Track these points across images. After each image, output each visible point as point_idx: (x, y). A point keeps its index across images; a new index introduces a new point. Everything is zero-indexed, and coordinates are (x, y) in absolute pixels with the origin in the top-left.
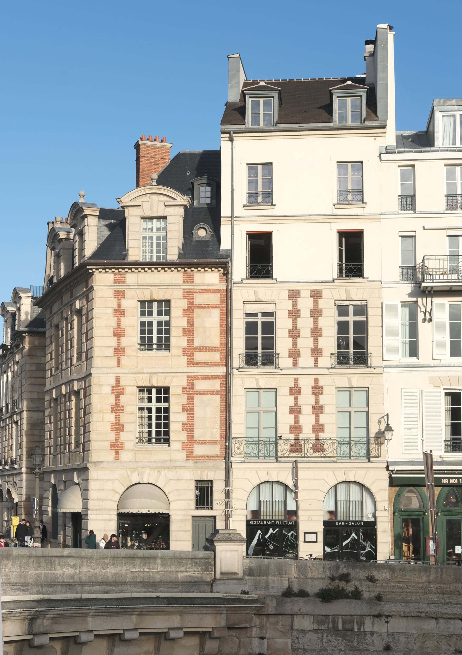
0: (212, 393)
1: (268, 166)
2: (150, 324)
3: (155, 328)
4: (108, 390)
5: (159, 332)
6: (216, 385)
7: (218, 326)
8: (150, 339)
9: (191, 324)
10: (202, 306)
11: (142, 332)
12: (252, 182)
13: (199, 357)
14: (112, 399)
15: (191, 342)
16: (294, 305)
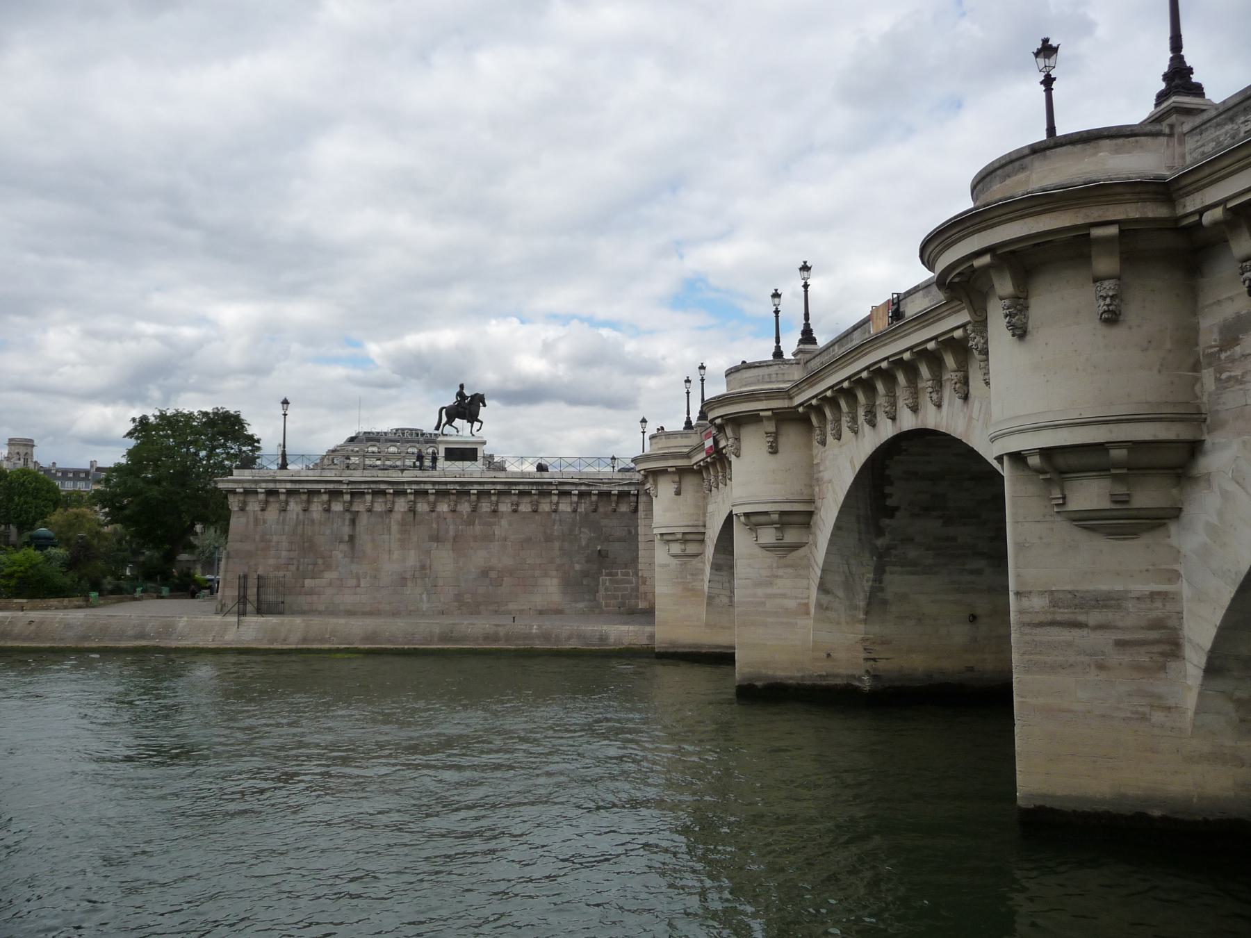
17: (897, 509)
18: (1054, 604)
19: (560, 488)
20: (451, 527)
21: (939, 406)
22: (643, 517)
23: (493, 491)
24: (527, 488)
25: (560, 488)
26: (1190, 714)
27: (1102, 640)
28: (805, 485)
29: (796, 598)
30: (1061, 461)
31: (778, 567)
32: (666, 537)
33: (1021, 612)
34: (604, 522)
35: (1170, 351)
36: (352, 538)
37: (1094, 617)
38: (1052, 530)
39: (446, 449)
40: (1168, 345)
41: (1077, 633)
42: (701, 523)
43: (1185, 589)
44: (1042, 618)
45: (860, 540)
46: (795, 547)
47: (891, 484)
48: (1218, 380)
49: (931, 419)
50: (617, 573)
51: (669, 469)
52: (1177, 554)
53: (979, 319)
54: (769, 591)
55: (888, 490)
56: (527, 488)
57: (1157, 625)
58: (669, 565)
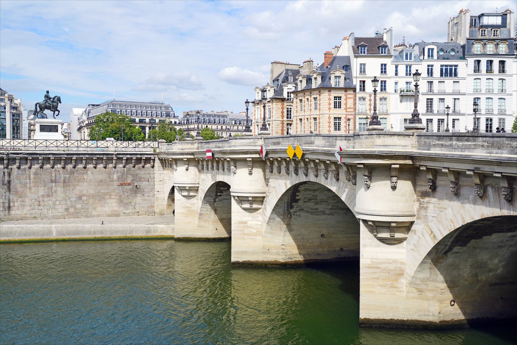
1: (364, 65)
2: (336, 102)
3: (338, 103)
4: (327, 118)
5: (339, 104)
7: (353, 103)
8: (336, 106)
9: (346, 102)
10: (349, 98)
11: (335, 104)
12: (361, 68)
14: (328, 120)
15: (346, 107)
16: (370, 98)
17: (299, 200)
19: (118, 156)
20: (62, 175)
21: (327, 179)
22: (157, 170)
23: (84, 158)
24: (101, 156)
25: (118, 156)
28: (263, 186)
30: (377, 224)
32: (180, 188)
34: (138, 172)
35: (408, 197)
36: (9, 182)
38: (373, 241)
39: (40, 125)
40: (408, 195)
45: (284, 209)
46: (257, 209)
47: (299, 192)
49: (322, 180)
51: (184, 159)
53: (354, 175)
55: (297, 194)
56: (101, 156)
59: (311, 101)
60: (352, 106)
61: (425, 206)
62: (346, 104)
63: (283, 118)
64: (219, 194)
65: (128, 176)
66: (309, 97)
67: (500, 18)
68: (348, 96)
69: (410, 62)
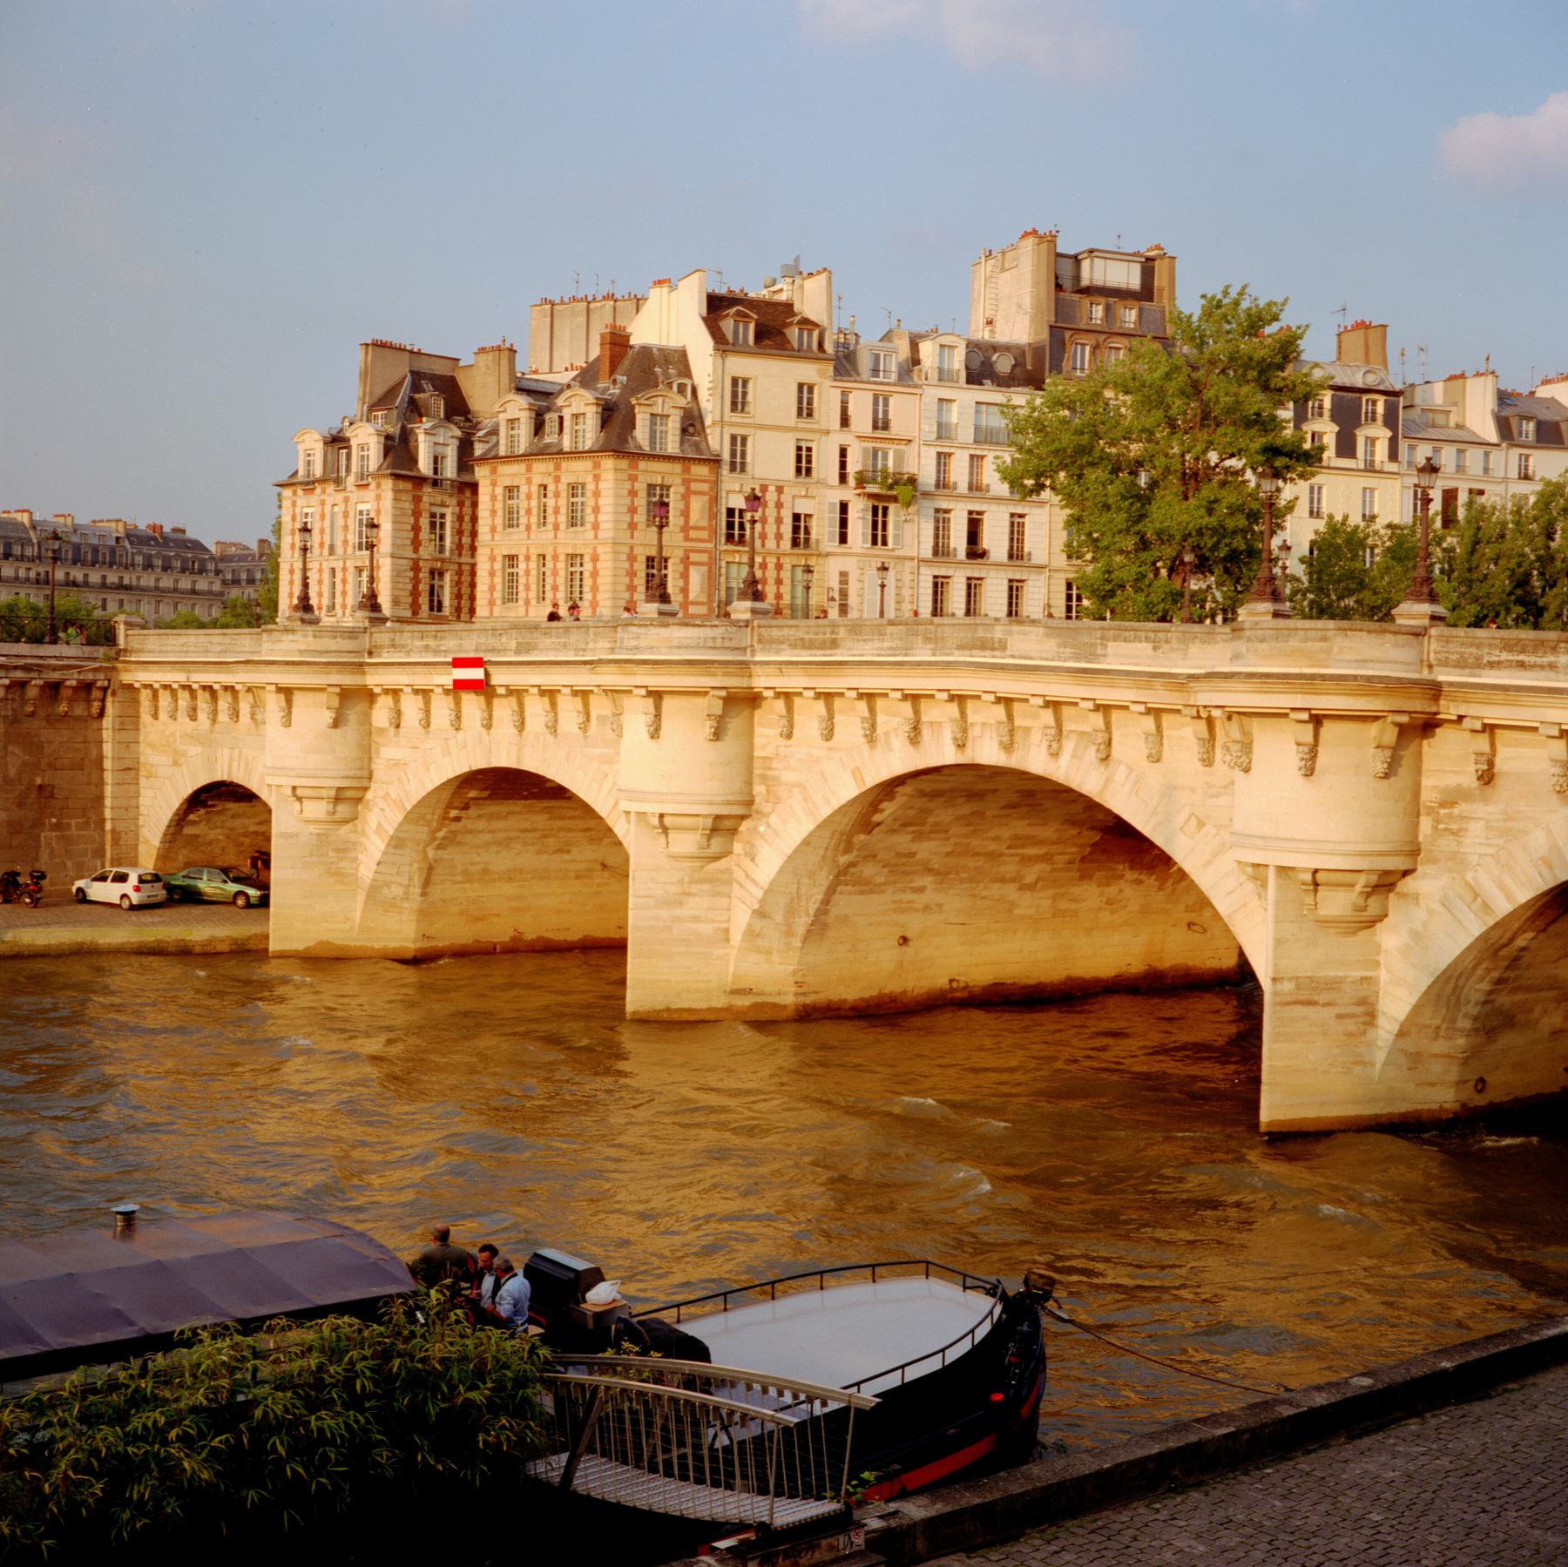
0: (701, 564)
6: (704, 558)
10: (696, 493)
13: (693, 534)
14: (627, 565)
18: (1298, 987)
26: (1378, 1066)
27: (1326, 1014)
29: (713, 921)
31: (691, 883)
33: (1275, 994)
37: (1323, 998)
41: (1311, 1009)
42: (365, 773)
43: (1383, 975)
44: (1289, 999)
48: (1435, 828)
50: (69, 825)
52: (1378, 948)
54: (677, 912)
57: (1362, 1002)
58: (297, 835)
59: (557, 495)
60: (705, 523)
61: (1454, 827)
62: (686, 513)
63: (416, 550)
64: (453, 813)
65: (11, 748)
66: (549, 481)
67: (1136, 270)
68: (694, 486)
69: (882, 383)
